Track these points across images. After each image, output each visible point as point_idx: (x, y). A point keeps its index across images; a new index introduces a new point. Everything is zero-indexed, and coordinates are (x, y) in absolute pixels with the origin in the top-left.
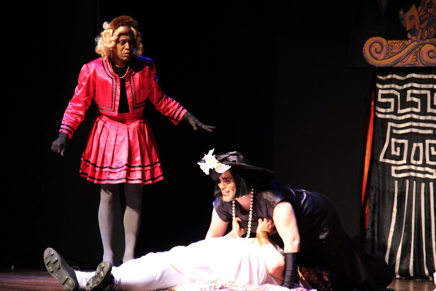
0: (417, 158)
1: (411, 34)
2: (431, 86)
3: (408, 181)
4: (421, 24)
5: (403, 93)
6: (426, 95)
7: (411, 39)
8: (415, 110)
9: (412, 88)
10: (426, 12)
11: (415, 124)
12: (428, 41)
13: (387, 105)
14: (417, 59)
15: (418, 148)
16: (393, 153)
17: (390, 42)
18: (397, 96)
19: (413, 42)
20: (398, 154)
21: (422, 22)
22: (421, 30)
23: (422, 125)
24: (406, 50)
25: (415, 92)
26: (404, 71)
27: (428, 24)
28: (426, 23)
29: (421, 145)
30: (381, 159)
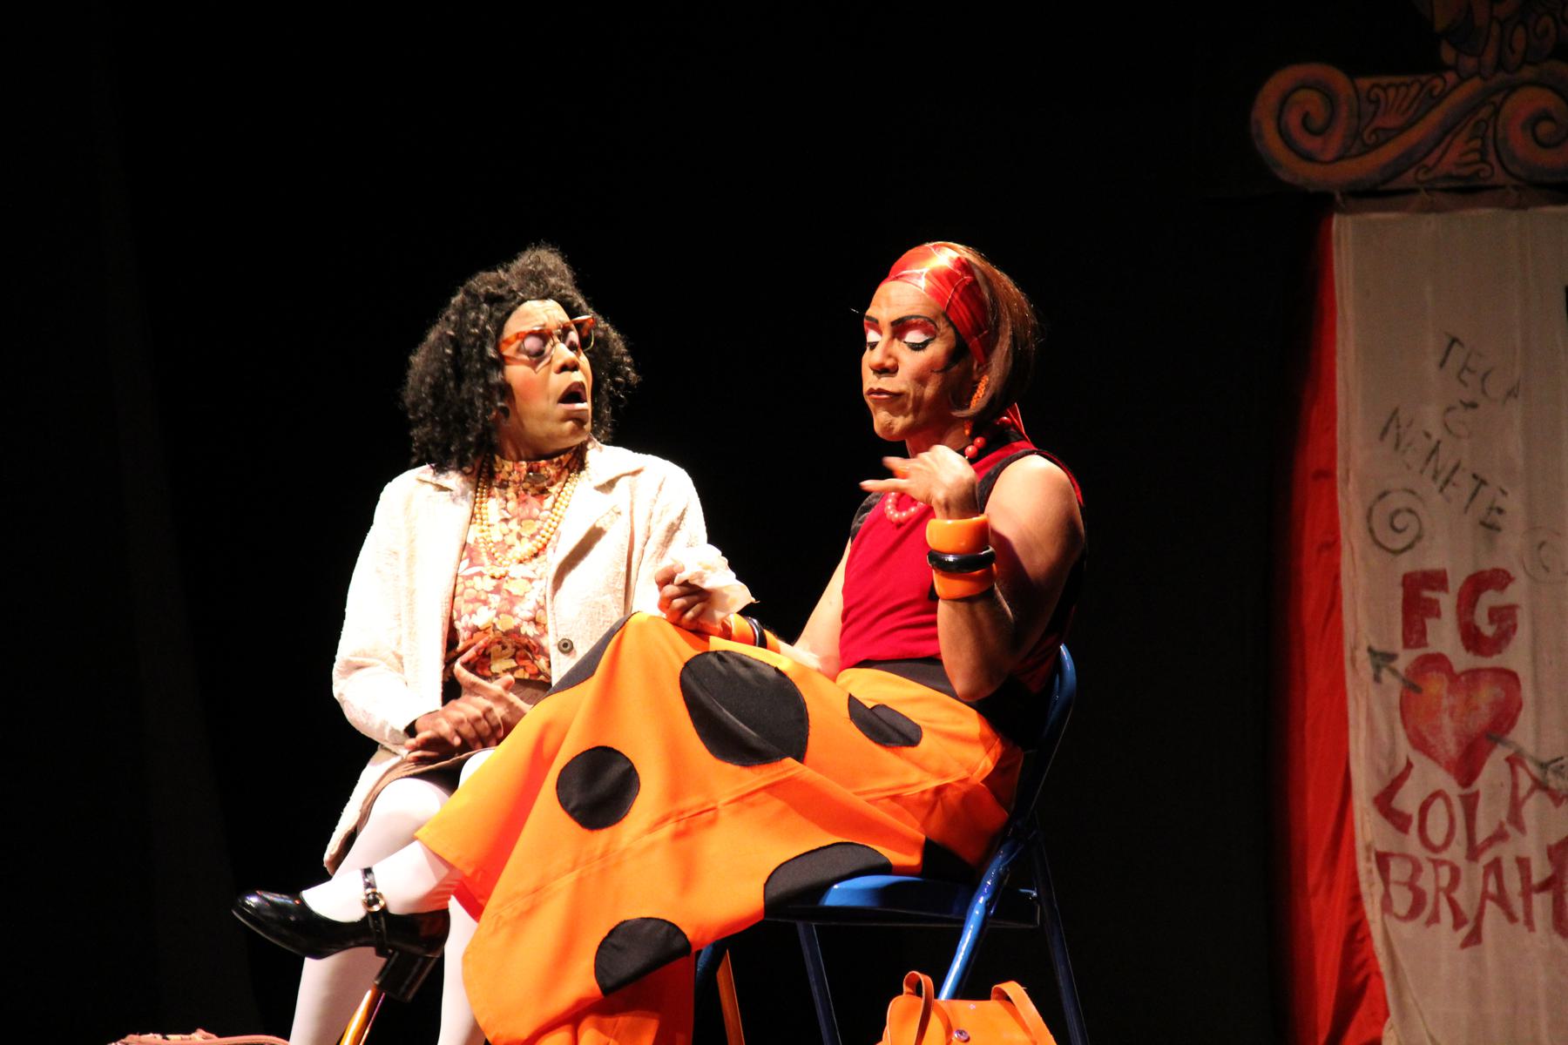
7: (1454, 68)
12: (1528, 72)
14: (1483, 152)
17: (1364, 83)
24: (1436, 116)
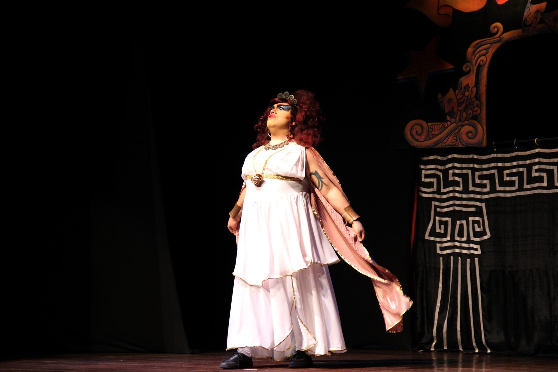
0: (461, 235)
1: (450, 116)
2: (471, 165)
3: (452, 257)
4: (458, 106)
5: (445, 172)
6: (467, 174)
7: (449, 121)
8: (457, 189)
9: (454, 168)
10: (464, 95)
11: (457, 202)
12: (466, 122)
13: (430, 185)
14: (456, 139)
15: (461, 226)
16: (438, 230)
17: (430, 124)
18: (440, 176)
19: (452, 124)
20: (442, 231)
21: (459, 104)
22: (459, 112)
23: (464, 202)
24: (446, 131)
25: (457, 171)
26: (445, 151)
27: (466, 107)
28: (464, 105)
29: (464, 222)
30: (427, 237)
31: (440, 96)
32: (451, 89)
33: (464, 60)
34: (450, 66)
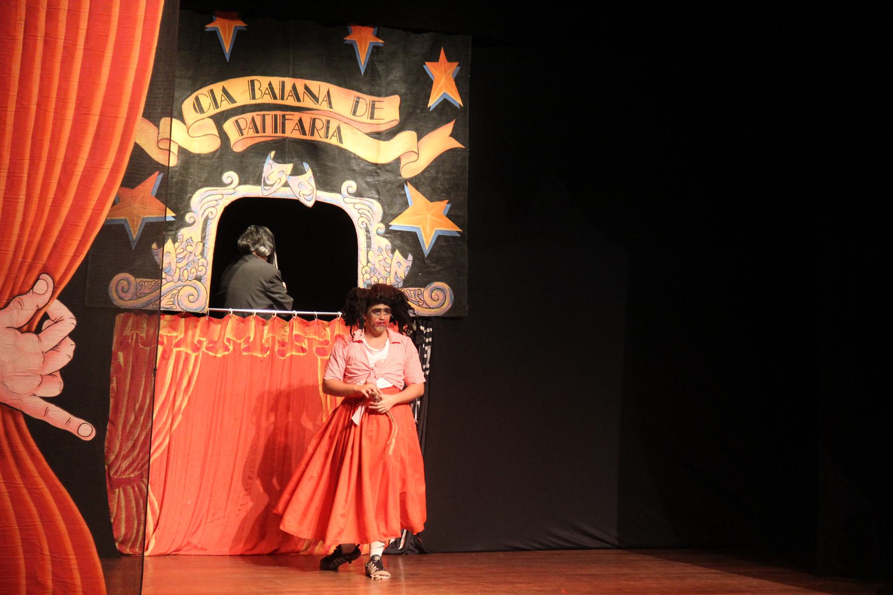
10: (185, 249)
17: (138, 280)
22: (178, 270)
31: (154, 246)
32: (170, 241)
33: (187, 208)
34: (170, 215)
